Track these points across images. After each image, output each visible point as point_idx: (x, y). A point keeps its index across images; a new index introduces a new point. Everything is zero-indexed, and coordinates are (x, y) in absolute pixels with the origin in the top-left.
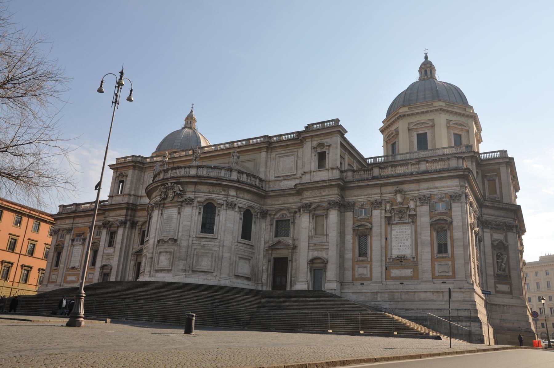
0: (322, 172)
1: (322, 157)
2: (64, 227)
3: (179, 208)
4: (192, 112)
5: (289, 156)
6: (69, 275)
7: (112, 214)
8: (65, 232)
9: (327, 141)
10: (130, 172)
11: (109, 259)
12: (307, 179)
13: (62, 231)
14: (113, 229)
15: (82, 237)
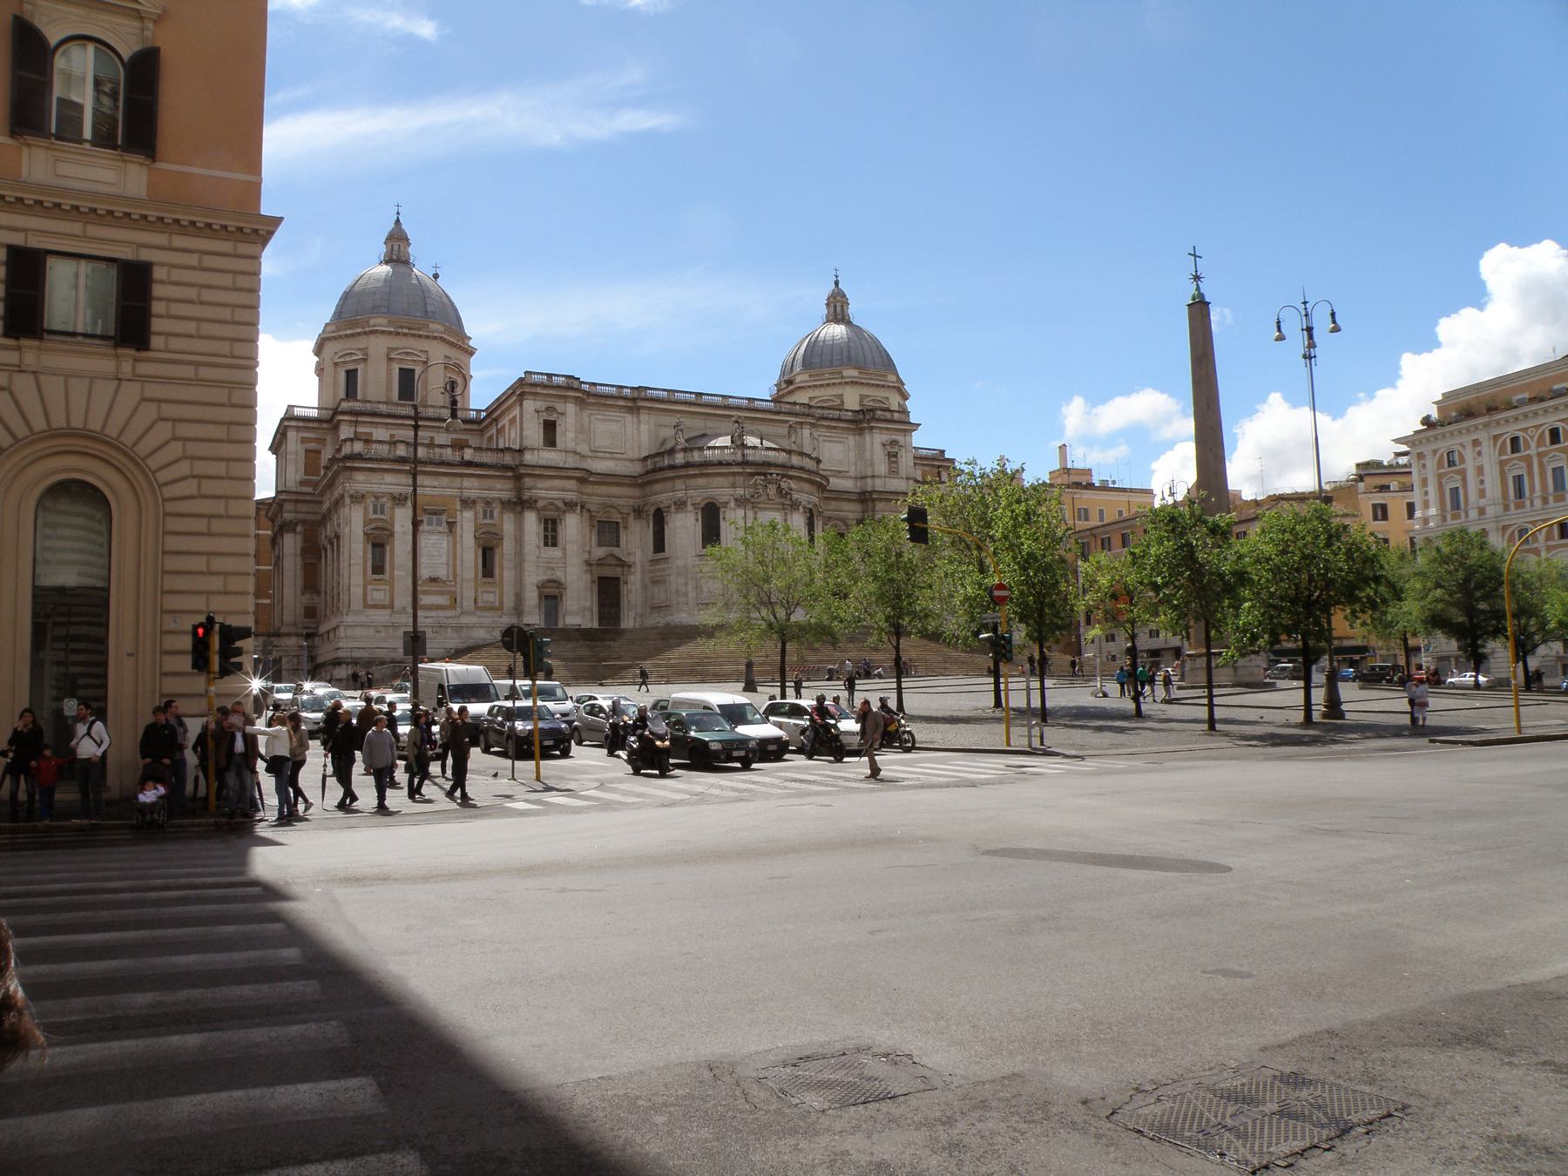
0: (896, 480)
1: (892, 457)
2: (381, 490)
3: (786, 514)
4: (398, 221)
5: (836, 442)
6: (426, 593)
7: (541, 484)
8: (384, 500)
9: (900, 438)
10: (571, 408)
11: (553, 569)
12: (879, 485)
13: (377, 498)
14: (551, 514)
15: (444, 518)
